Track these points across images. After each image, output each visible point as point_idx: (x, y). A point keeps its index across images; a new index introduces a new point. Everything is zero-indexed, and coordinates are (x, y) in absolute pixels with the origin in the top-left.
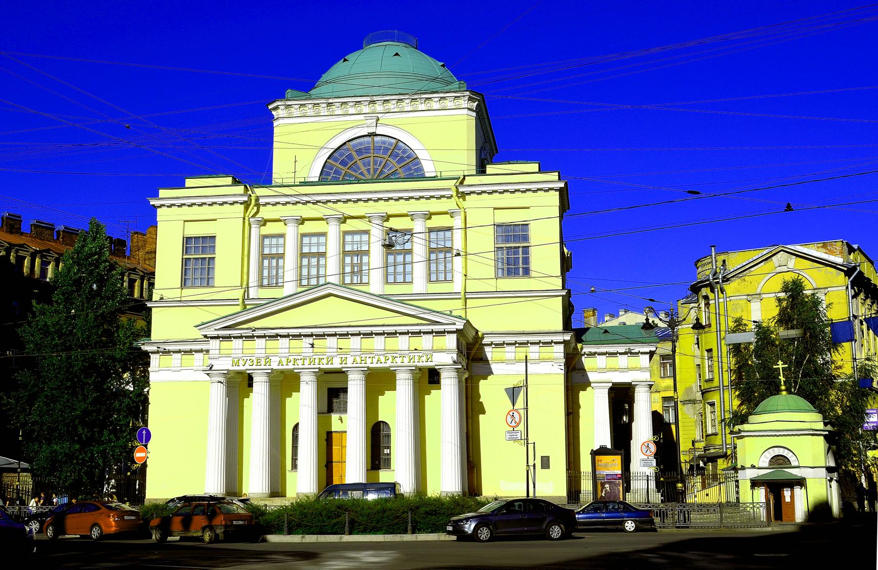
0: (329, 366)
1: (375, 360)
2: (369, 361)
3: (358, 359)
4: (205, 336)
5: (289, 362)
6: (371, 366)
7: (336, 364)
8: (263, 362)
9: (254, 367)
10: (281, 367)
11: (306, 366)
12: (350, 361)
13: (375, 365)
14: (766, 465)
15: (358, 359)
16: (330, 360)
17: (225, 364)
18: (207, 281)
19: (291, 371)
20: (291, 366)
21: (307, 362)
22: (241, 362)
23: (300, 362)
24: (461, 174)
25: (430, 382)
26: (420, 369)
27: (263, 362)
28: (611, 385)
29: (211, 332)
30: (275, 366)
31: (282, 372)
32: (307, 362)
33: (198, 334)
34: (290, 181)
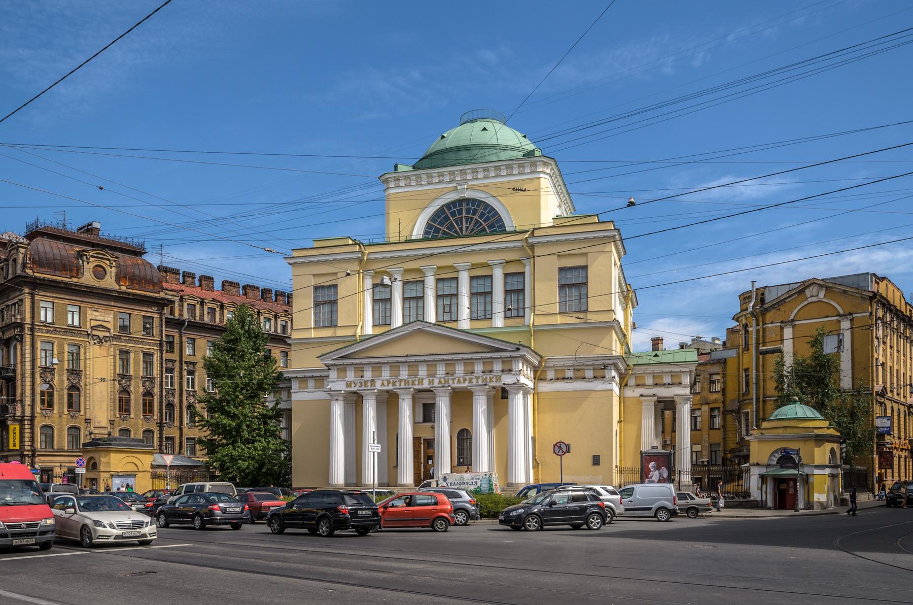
1: (456, 381)
2: (451, 382)
3: (443, 381)
4: (327, 366)
5: (389, 383)
7: (426, 385)
8: (369, 384)
9: (363, 388)
10: (383, 388)
11: (403, 386)
13: (456, 385)
14: (775, 463)
15: (443, 381)
16: (421, 381)
17: (341, 386)
20: (390, 387)
21: (403, 384)
22: (353, 385)
23: (398, 384)
24: (531, 228)
25: (502, 398)
26: (494, 388)
27: (369, 384)
29: (330, 362)
30: (378, 385)
31: (388, 391)
32: (403, 384)
33: (320, 364)
34: (396, 240)
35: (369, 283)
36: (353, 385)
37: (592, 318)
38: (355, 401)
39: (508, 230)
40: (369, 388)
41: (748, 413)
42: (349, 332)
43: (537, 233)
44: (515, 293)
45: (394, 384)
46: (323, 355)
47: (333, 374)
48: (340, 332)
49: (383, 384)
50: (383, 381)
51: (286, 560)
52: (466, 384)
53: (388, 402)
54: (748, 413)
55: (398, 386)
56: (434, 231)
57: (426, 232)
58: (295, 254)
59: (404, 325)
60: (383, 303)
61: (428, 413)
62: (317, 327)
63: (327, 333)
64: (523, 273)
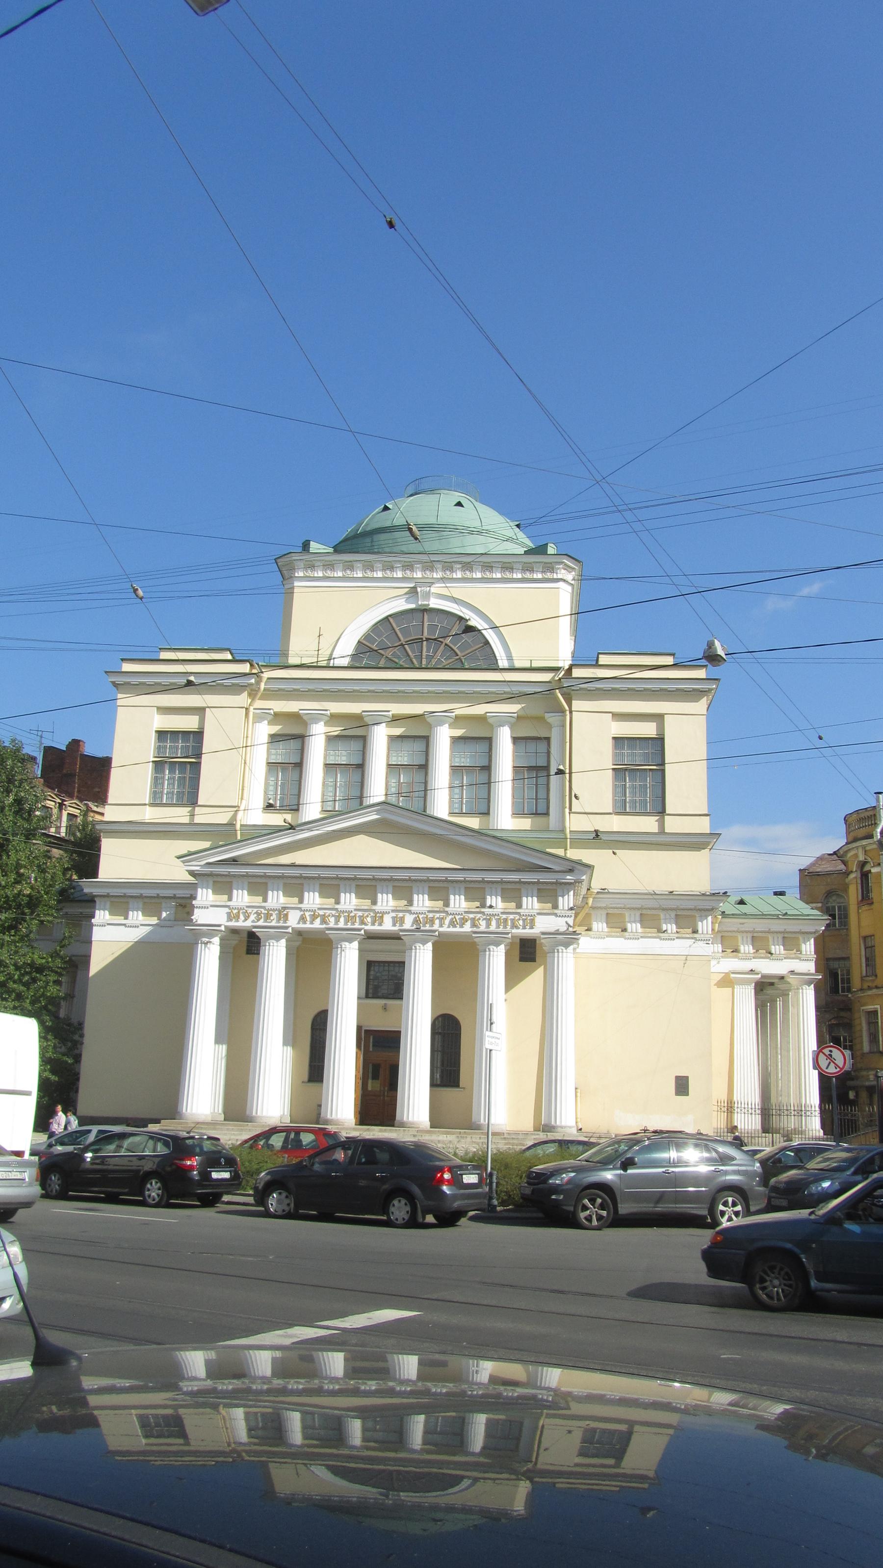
0: (376, 927)
4: (192, 873)
6: (441, 929)
7: (388, 925)
10: (301, 926)
11: (341, 924)
12: (408, 924)
16: (378, 918)
18: (189, 796)
19: (321, 932)
20: (317, 924)
22: (242, 917)
28: (759, 976)
30: (293, 921)
33: (179, 874)
35: (264, 730)
36: (242, 917)
37: (672, 825)
38: (246, 946)
39: (503, 663)
40: (273, 924)
41: (875, 1012)
42: (222, 818)
43: (577, 673)
44: (541, 772)
45: (324, 921)
46: (190, 854)
47: (205, 895)
48: (203, 817)
49: (303, 919)
50: (311, 909)
51: (568, 1483)
52: (467, 928)
53: (311, 954)
54: (875, 1012)
55: (332, 925)
56: (372, 651)
57: (354, 656)
58: (127, 667)
59: (330, 815)
60: (290, 769)
61: (384, 980)
62: (156, 802)
63: (179, 815)
64: (548, 739)
